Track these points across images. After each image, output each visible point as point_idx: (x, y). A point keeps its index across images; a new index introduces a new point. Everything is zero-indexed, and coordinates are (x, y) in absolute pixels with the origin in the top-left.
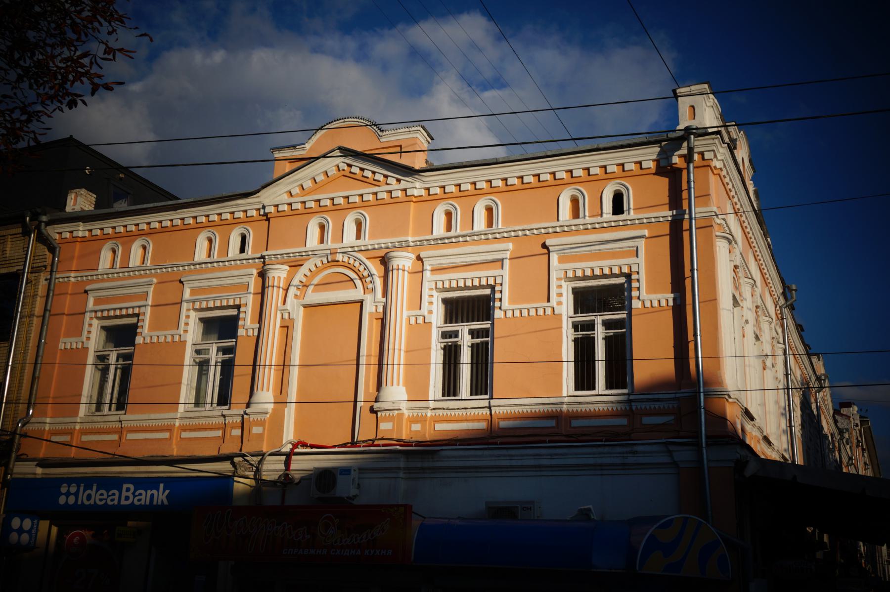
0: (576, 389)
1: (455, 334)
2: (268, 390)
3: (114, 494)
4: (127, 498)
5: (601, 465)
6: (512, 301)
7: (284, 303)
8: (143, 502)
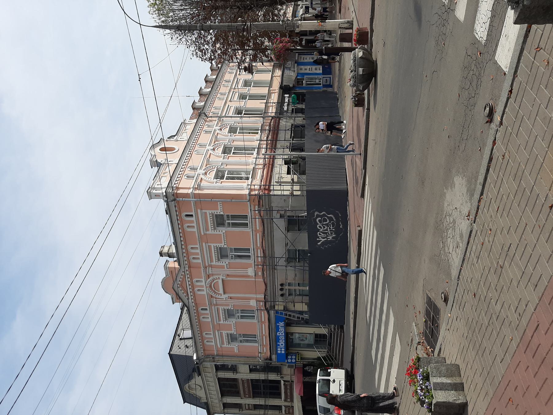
0: (248, 228)
2: (250, 302)
3: (281, 338)
4: (282, 334)
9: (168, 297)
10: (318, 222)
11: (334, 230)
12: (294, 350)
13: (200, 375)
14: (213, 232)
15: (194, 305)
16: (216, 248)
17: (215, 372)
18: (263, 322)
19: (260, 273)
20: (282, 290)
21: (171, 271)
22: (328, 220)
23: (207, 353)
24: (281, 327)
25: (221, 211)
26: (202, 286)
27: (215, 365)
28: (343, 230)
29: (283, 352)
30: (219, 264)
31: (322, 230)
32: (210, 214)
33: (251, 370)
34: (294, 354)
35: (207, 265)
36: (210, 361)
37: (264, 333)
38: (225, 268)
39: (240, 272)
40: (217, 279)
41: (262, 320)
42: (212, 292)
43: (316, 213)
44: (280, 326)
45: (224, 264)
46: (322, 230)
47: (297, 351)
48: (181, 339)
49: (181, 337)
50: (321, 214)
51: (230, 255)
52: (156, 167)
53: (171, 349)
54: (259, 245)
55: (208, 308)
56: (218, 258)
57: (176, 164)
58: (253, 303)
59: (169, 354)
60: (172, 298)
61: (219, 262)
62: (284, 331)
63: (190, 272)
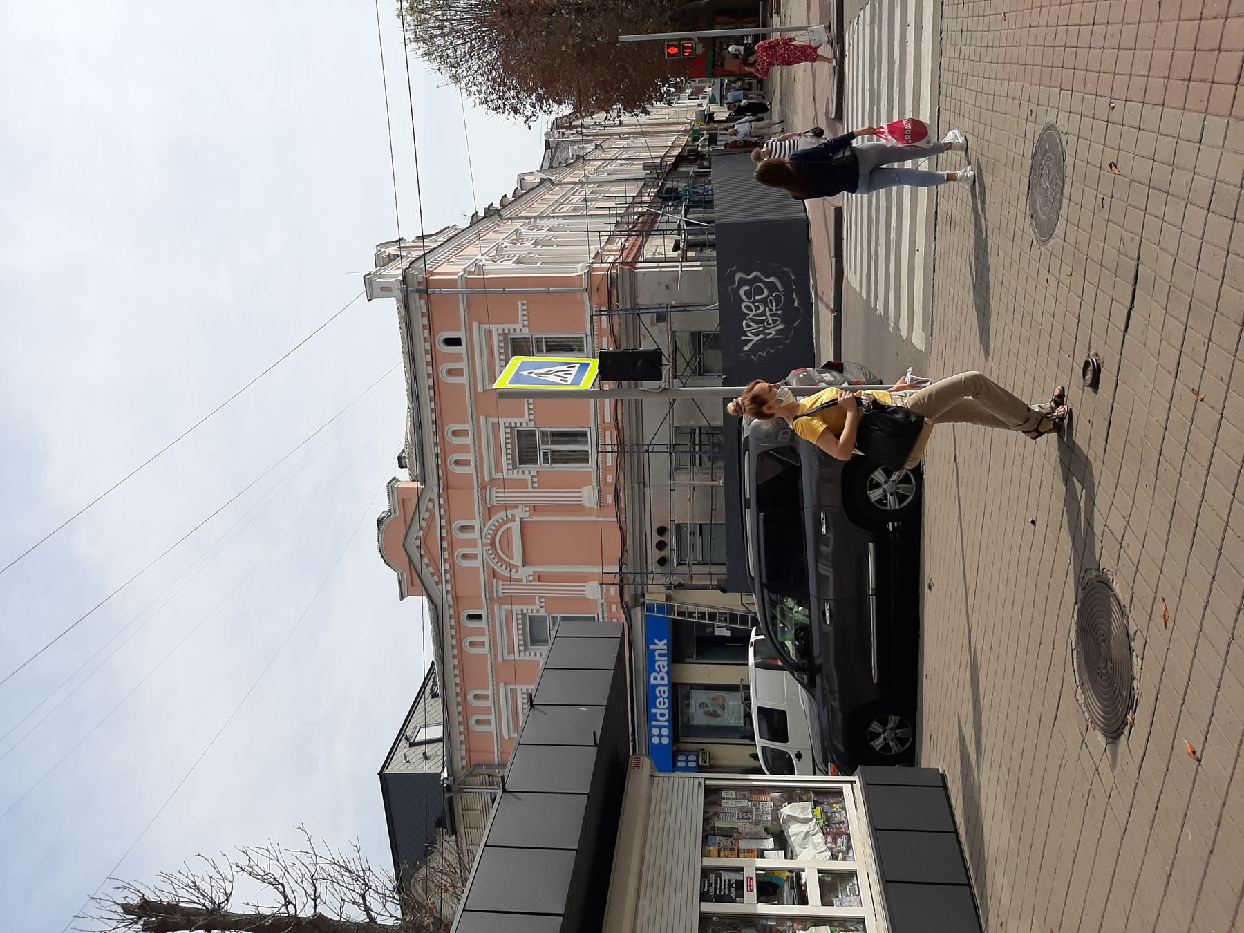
1: (545, 454)
2: (584, 586)
3: (660, 692)
7: (521, 580)
9: (390, 578)
10: (744, 297)
11: (780, 312)
12: (692, 744)
15: (451, 603)
19: (610, 499)
20: (661, 546)
21: (403, 500)
22: (765, 291)
23: (476, 758)
24: (660, 655)
25: (524, 326)
26: (472, 543)
28: (802, 311)
29: (665, 741)
30: (516, 477)
31: (754, 315)
35: (487, 479)
38: (528, 489)
39: (564, 497)
42: (493, 556)
43: (739, 276)
44: (657, 653)
45: (527, 477)
46: (754, 315)
47: (699, 747)
50: (750, 277)
51: (542, 451)
53: (386, 764)
54: (607, 420)
56: (514, 462)
58: (592, 590)
60: (400, 582)
61: (515, 471)
62: (666, 669)
63: (447, 500)
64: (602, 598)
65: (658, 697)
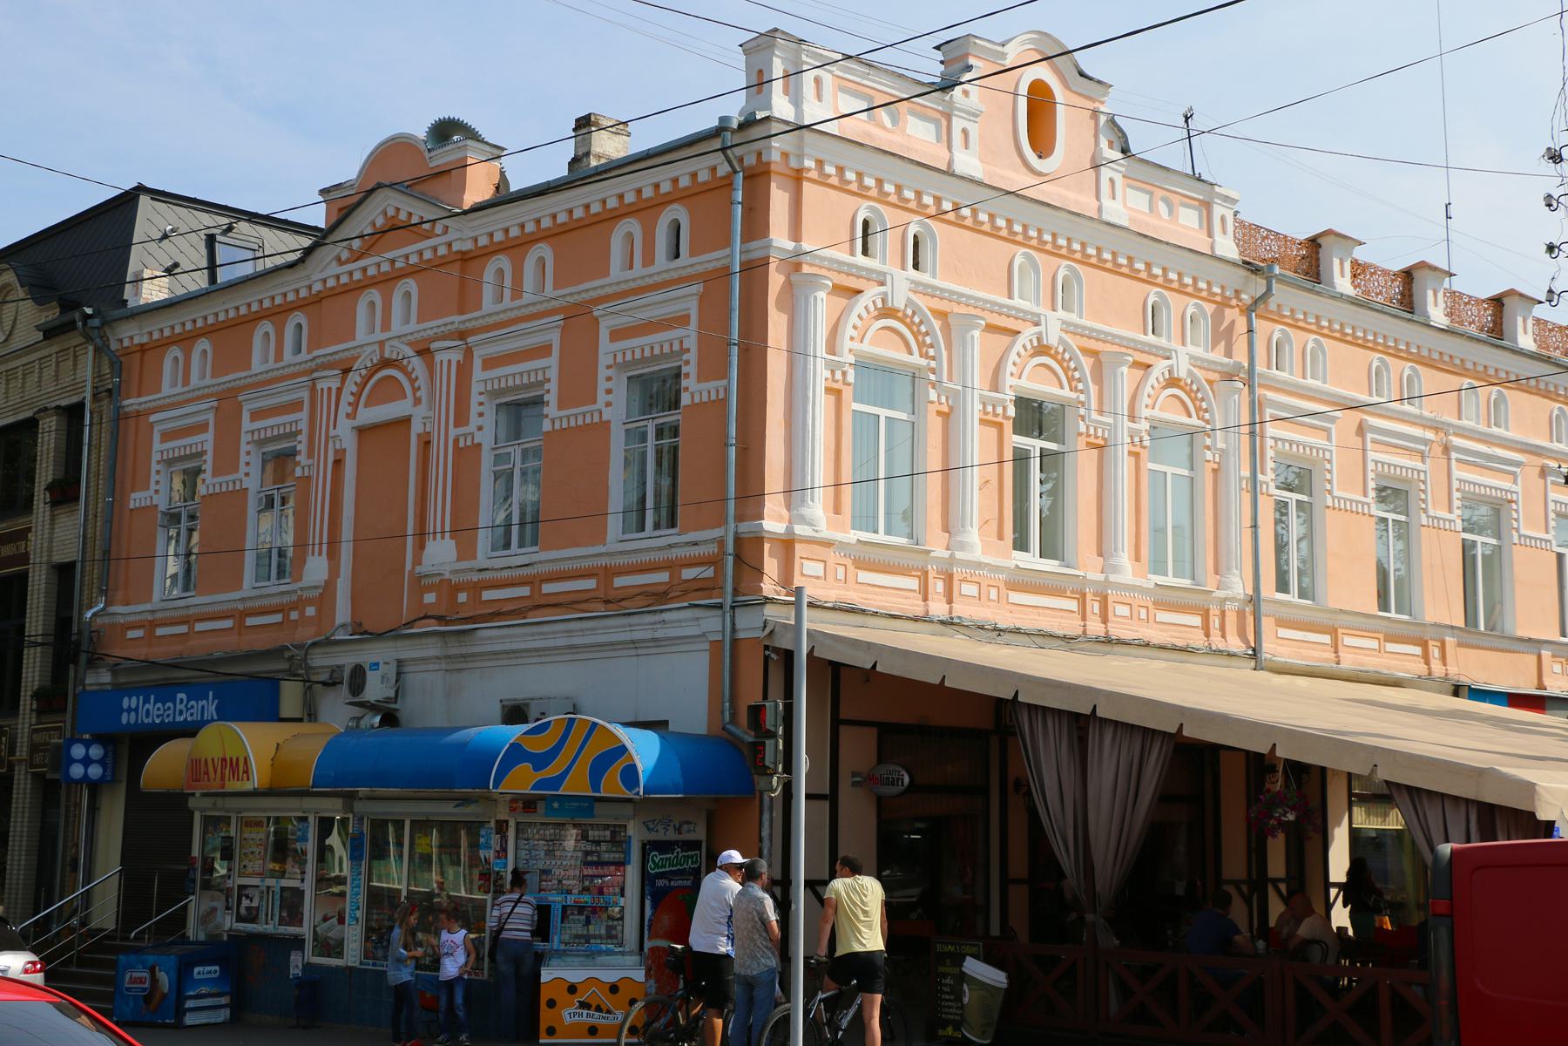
5: (633, 642)
6: (562, 405)
8: (194, 718)
13: (46, 337)
14: (604, 360)
16: (540, 378)
17: (58, 403)
18: (241, 623)
27: (80, 406)
30: (475, 399)
32: (681, 342)
33: (64, 573)
34: (109, 773)
36: (98, 375)
37: (199, 627)
38: (457, 425)
40: (415, 390)
41: (250, 615)
45: (474, 421)
48: (211, 241)
49: (219, 238)
52: (942, 67)
53: (159, 195)
55: (304, 356)
57: (944, 168)
59: (141, 189)
64: (301, 589)
65: (164, 705)
